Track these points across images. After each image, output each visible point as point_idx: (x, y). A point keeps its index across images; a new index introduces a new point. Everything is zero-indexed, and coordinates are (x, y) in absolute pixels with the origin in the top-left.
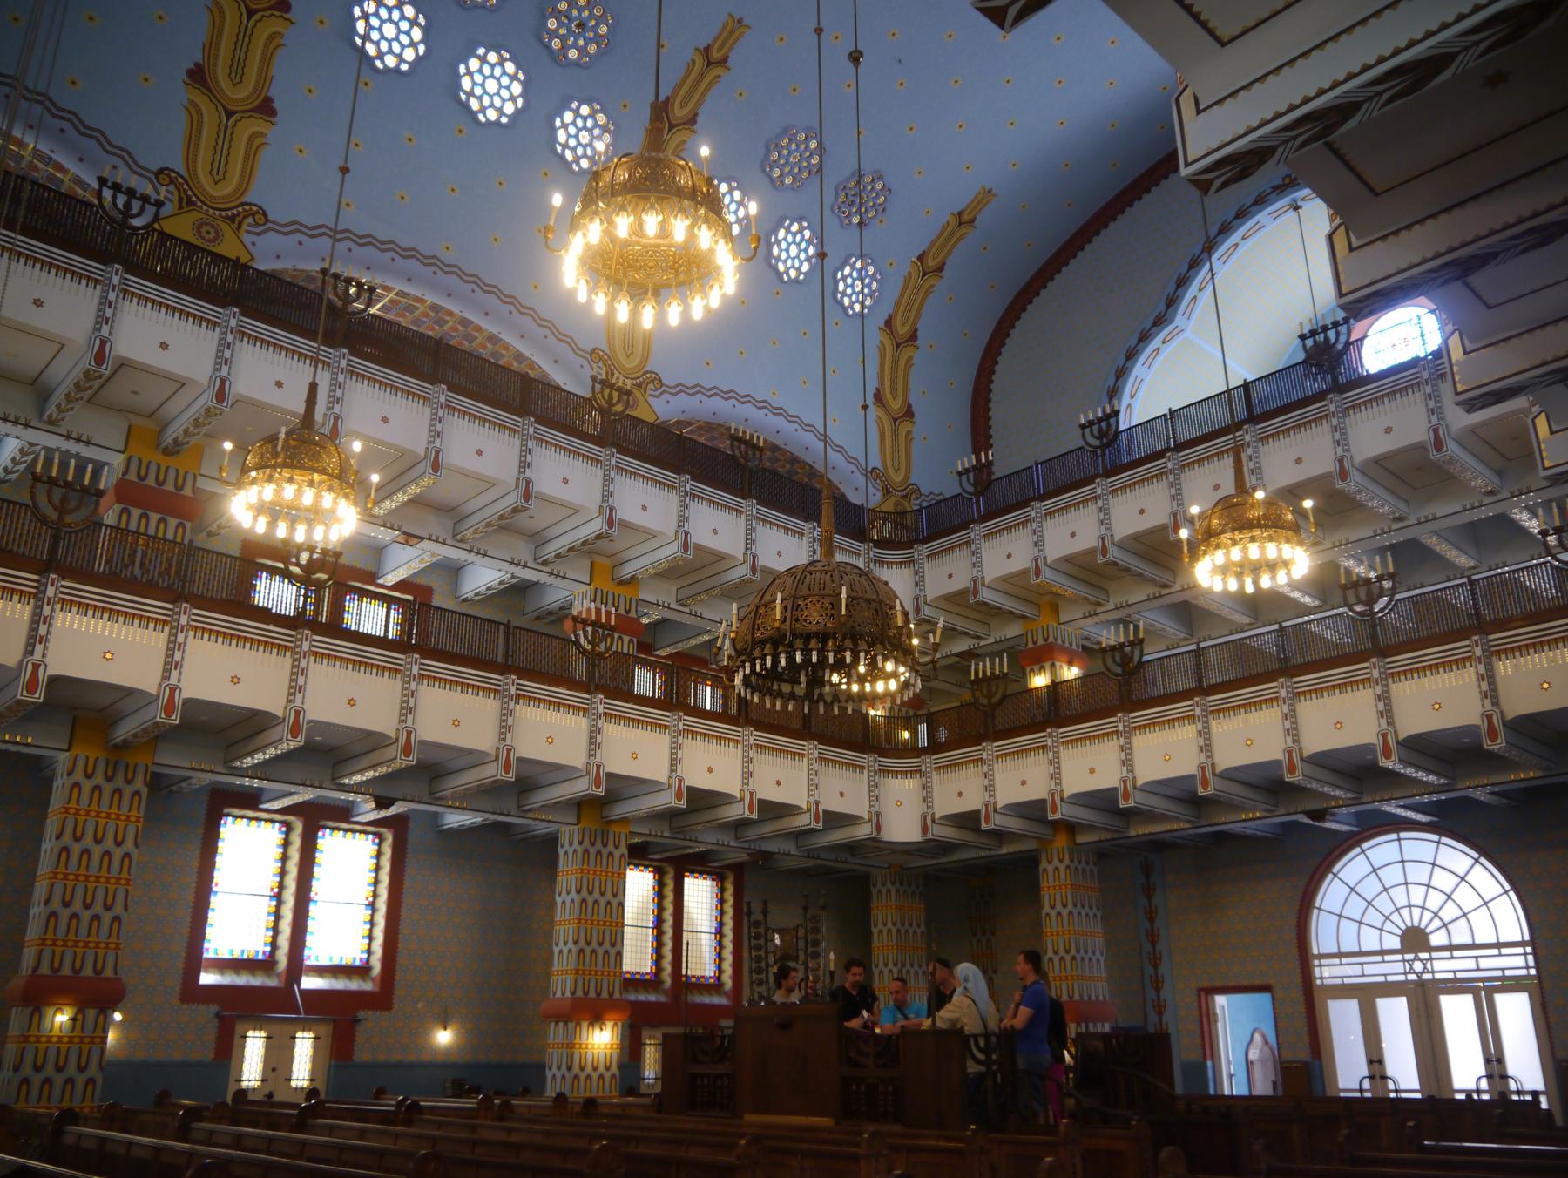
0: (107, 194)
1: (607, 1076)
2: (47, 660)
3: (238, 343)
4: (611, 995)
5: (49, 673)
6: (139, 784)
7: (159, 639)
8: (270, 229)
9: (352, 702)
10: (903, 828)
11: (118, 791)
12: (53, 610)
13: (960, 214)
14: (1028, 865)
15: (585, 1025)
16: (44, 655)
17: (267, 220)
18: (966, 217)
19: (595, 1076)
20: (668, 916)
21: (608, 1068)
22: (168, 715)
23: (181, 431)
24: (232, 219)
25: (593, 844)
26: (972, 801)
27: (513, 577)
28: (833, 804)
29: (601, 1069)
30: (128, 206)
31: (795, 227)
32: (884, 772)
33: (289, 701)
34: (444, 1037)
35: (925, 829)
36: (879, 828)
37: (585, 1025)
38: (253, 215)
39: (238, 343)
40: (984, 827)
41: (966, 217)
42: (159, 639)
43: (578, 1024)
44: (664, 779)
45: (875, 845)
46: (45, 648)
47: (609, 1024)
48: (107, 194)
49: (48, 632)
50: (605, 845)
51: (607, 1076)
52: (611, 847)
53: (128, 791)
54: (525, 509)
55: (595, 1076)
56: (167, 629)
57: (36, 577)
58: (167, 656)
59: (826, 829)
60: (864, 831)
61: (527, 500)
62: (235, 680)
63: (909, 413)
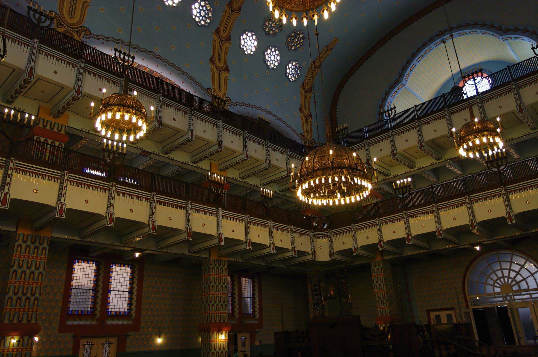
0: (31, 13)
1: (224, 352)
2: (10, 192)
3: (84, 73)
4: (224, 321)
5: (11, 197)
6: (45, 245)
7: (56, 185)
8: (92, 37)
9: (131, 211)
10: (323, 256)
11: (37, 247)
12: (12, 172)
13: (327, 46)
14: (366, 269)
15: (215, 333)
16: (9, 190)
17: (90, 34)
18: (329, 48)
19: (220, 352)
20: (236, 292)
21: (224, 349)
22: (61, 215)
23: (61, 107)
24: (77, 32)
25: (215, 265)
26: (349, 245)
27: (183, 168)
28: (300, 248)
29: (222, 349)
30: (40, 18)
31: (273, 50)
32: (315, 237)
33: (107, 210)
34: (159, 341)
35: (331, 256)
36: (315, 256)
37: (215, 333)
38: (85, 31)
39: (84, 73)
40: (354, 254)
41: (329, 48)
42: (56, 185)
43: (213, 333)
44: (243, 239)
45: (314, 263)
46: (9, 187)
47: (224, 332)
48: (31, 13)
49: (10, 181)
50: (220, 265)
51: (224, 352)
52: (222, 266)
53: (41, 247)
54: (191, 141)
55: (220, 352)
56: (59, 181)
57: (5, 159)
58: (59, 191)
59: (299, 257)
60: (310, 257)
61: (192, 137)
62: (87, 201)
63: (310, 116)
